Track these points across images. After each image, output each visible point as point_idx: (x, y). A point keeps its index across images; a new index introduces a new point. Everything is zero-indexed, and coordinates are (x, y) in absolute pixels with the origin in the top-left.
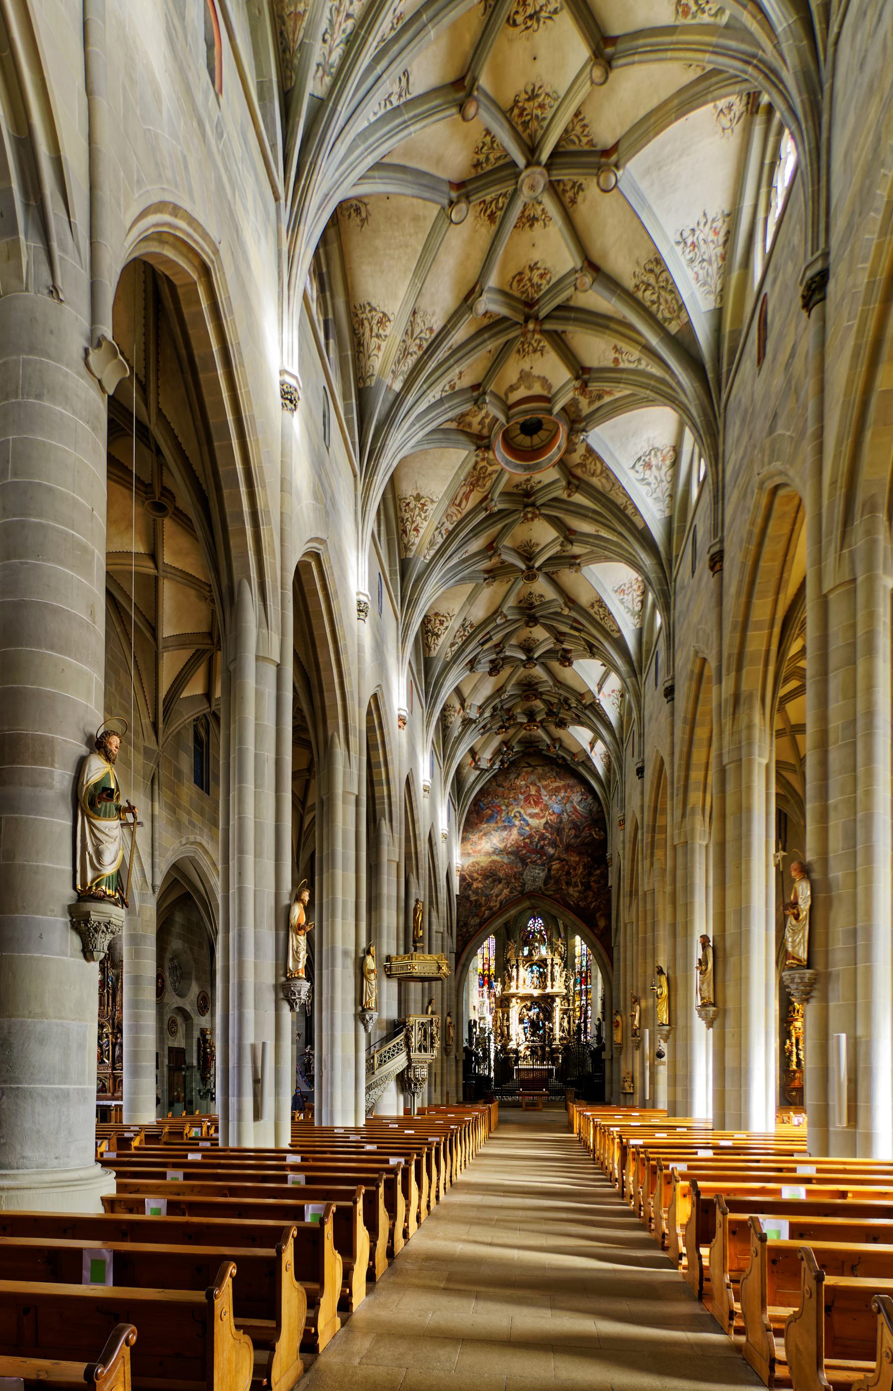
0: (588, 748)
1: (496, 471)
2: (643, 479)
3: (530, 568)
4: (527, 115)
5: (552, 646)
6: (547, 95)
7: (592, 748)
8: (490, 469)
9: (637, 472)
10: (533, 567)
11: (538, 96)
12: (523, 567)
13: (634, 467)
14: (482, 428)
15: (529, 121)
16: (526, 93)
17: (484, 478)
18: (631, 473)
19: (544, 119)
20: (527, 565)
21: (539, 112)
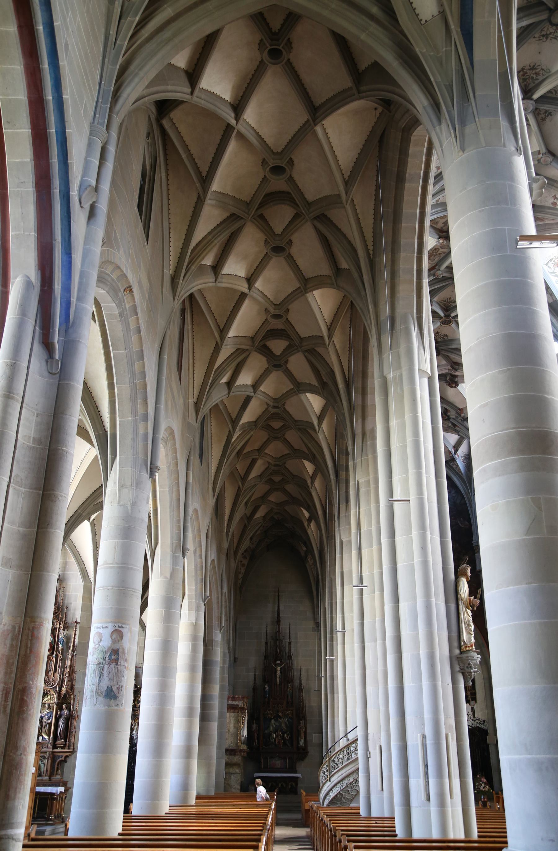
0: (453, 451)
1: (445, 253)
2: (553, 273)
3: (447, 316)
4: (527, 76)
5: (447, 371)
6: (543, 70)
7: (456, 451)
8: (441, 250)
9: (549, 267)
10: (449, 316)
11: (536, 69)
12: (442, 314)
13: (547, 264)
14: (444, 226)
15: (527, 78)
16: (530, 66)
17: (435, 256)
18: (546, 268)
19: (537, 79)
20: (444, 314)
21: (534, 76)
